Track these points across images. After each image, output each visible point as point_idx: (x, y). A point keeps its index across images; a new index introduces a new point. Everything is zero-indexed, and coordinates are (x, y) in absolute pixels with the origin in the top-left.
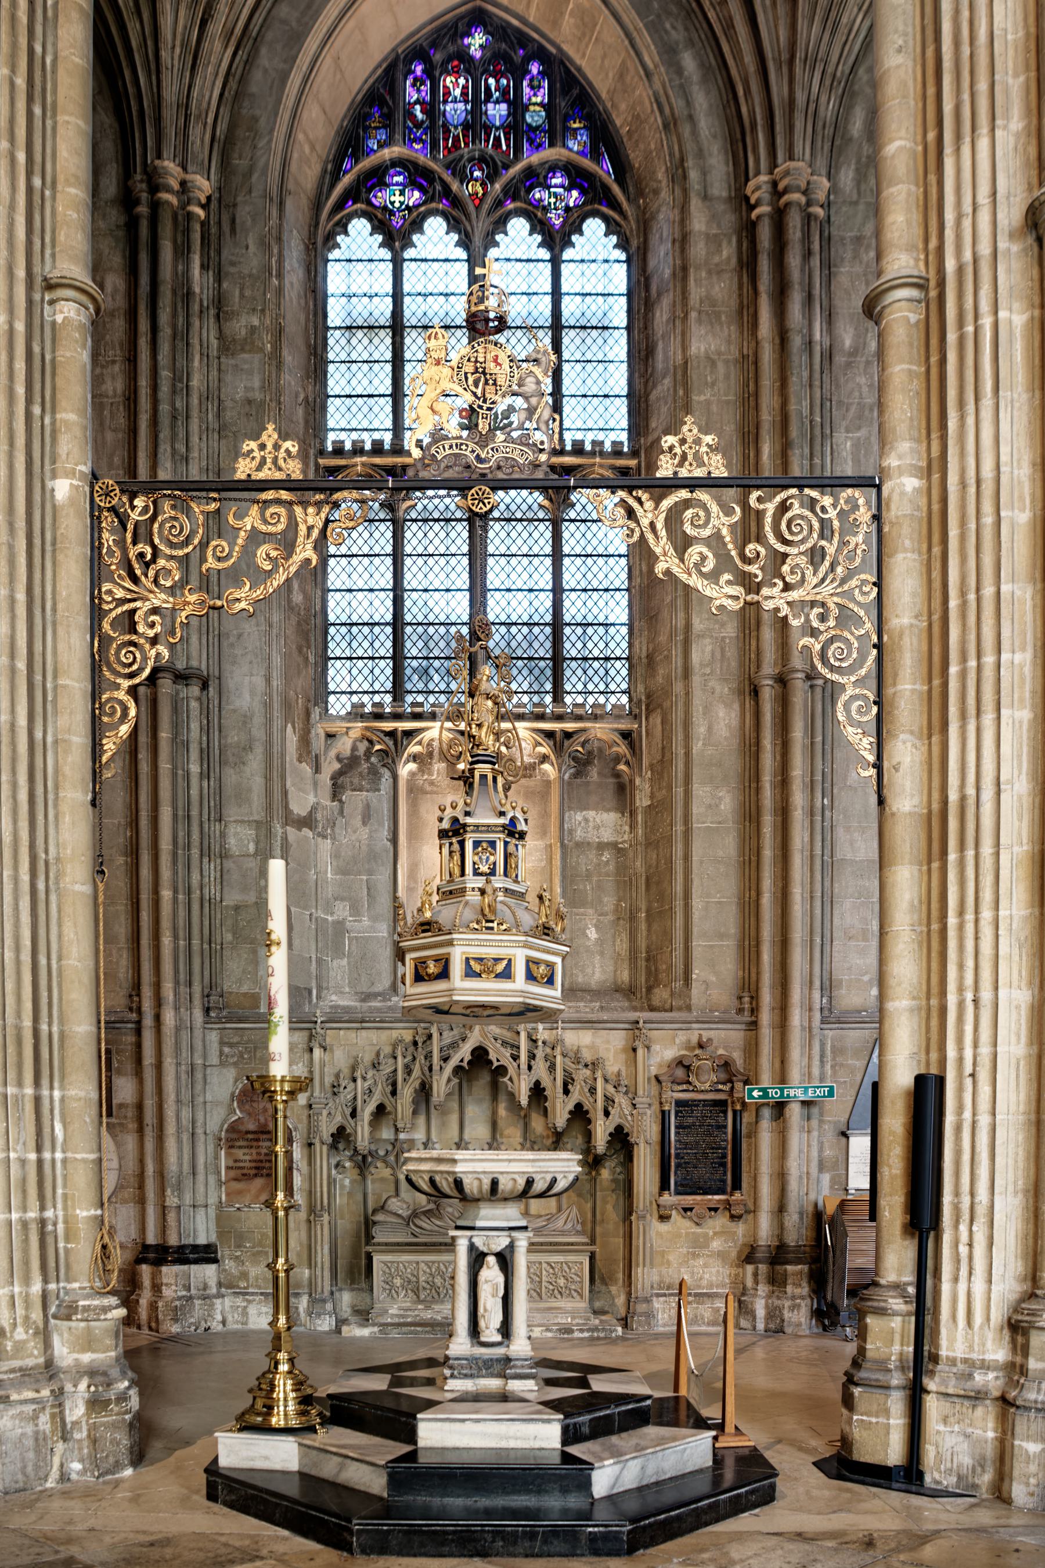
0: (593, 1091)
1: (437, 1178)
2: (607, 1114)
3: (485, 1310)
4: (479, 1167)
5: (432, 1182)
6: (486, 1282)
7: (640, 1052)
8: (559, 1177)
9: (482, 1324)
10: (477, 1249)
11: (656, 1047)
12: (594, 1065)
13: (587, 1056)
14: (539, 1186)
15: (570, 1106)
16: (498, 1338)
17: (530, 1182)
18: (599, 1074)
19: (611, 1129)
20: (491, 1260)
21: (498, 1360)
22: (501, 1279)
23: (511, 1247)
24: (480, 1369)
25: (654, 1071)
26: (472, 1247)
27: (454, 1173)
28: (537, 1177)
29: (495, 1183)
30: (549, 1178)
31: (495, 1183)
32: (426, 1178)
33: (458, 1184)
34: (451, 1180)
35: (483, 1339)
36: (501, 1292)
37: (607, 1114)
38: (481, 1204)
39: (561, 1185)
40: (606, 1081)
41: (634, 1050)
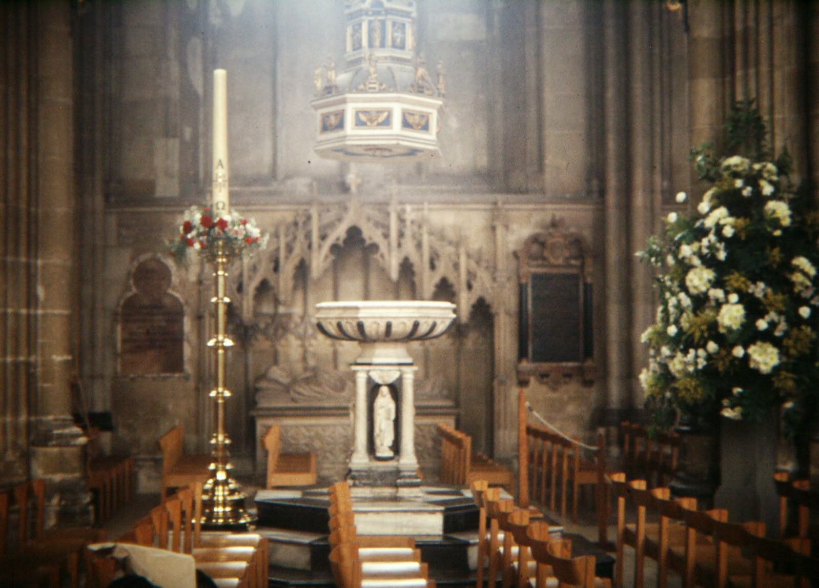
0: (456, 266)
1: (344, 323)
2: (470, 287)
3: (381, 431)
4: (377, 313)
5: (339, 326)
6: (382, 407)
7: (500, 231)
8: (438, 322)
9: (378, 442)
10: (373, 381)
11: (514, 227)
12: (457, 245)
13: (451, 235)
14: (423, 329)
15: (437, 279)
16: (390, 454)
17: (416, 325)
18: (462, 251)
19: (473, 301)
20: (385, 390)
21: (391, 473)
22: (392, 405)
23: (400, 380)
24: (376, 480)
25: (512, 247)
26: (369, 380)
27: (357, 318)
28: (422, 321)
29: (389, 326)
30: (430, 322)
31: (389, 326)
32: (334, 322)
33: (360, 326)
34: (354, 323)
35: (379, 454)
36: (393, 416)
37: (470, 287)
38: (377, 345)
39: (441, 328)
40: (469, 256)
41: (493, 228)
